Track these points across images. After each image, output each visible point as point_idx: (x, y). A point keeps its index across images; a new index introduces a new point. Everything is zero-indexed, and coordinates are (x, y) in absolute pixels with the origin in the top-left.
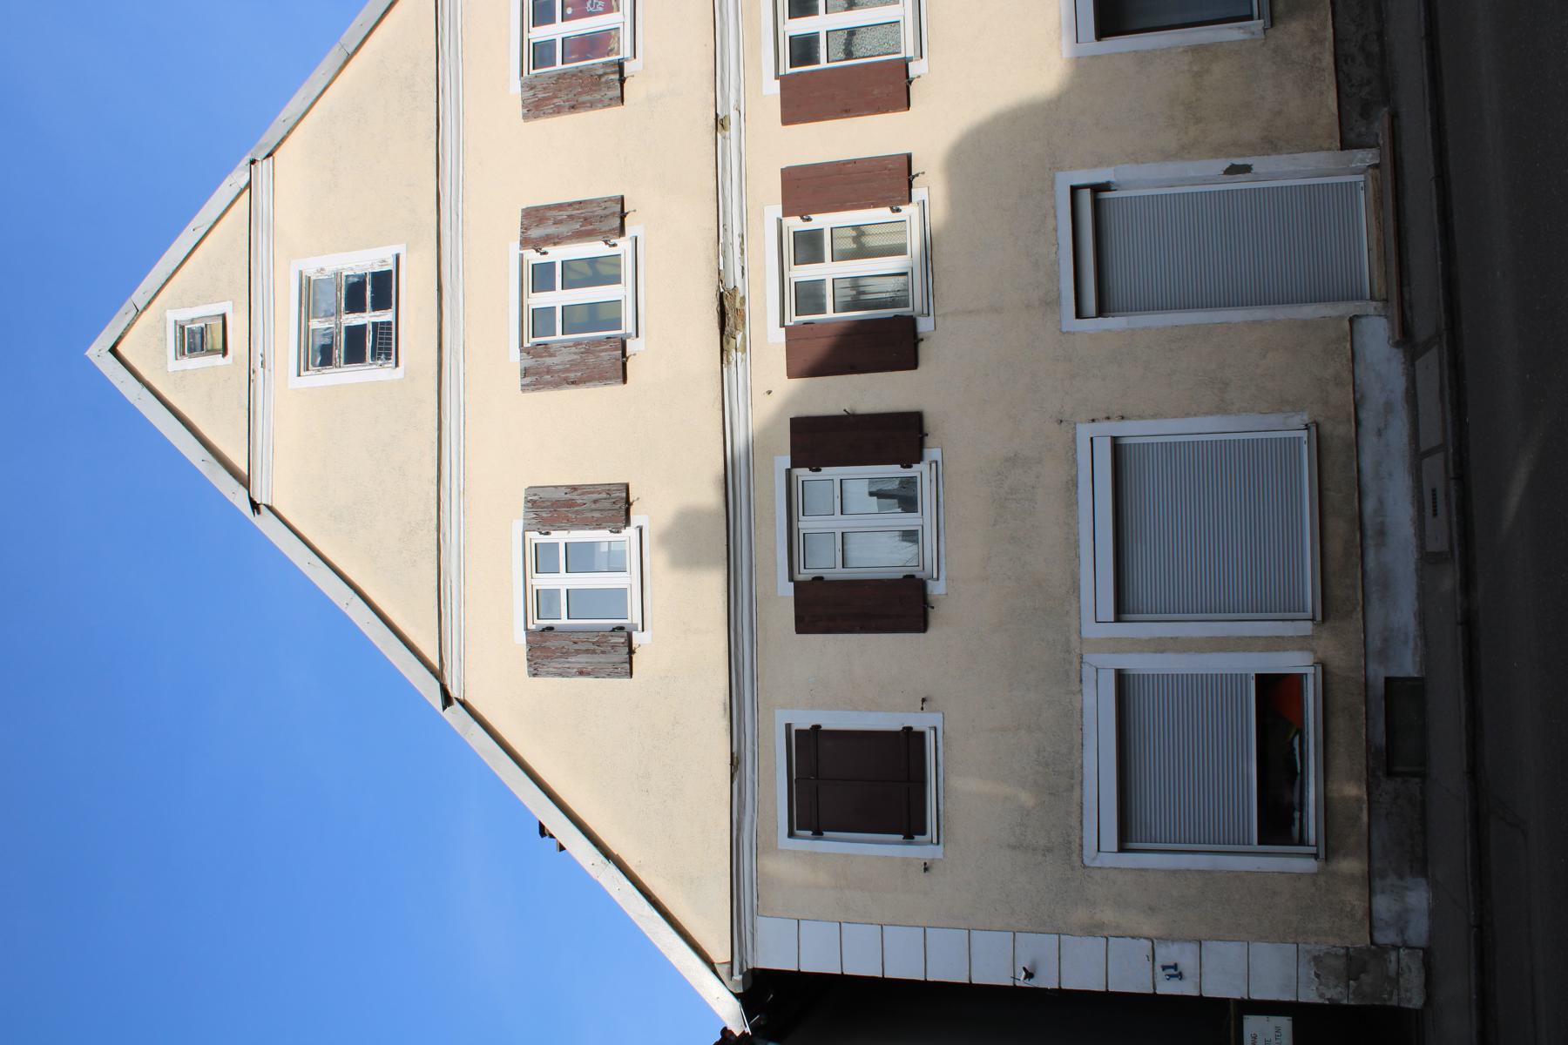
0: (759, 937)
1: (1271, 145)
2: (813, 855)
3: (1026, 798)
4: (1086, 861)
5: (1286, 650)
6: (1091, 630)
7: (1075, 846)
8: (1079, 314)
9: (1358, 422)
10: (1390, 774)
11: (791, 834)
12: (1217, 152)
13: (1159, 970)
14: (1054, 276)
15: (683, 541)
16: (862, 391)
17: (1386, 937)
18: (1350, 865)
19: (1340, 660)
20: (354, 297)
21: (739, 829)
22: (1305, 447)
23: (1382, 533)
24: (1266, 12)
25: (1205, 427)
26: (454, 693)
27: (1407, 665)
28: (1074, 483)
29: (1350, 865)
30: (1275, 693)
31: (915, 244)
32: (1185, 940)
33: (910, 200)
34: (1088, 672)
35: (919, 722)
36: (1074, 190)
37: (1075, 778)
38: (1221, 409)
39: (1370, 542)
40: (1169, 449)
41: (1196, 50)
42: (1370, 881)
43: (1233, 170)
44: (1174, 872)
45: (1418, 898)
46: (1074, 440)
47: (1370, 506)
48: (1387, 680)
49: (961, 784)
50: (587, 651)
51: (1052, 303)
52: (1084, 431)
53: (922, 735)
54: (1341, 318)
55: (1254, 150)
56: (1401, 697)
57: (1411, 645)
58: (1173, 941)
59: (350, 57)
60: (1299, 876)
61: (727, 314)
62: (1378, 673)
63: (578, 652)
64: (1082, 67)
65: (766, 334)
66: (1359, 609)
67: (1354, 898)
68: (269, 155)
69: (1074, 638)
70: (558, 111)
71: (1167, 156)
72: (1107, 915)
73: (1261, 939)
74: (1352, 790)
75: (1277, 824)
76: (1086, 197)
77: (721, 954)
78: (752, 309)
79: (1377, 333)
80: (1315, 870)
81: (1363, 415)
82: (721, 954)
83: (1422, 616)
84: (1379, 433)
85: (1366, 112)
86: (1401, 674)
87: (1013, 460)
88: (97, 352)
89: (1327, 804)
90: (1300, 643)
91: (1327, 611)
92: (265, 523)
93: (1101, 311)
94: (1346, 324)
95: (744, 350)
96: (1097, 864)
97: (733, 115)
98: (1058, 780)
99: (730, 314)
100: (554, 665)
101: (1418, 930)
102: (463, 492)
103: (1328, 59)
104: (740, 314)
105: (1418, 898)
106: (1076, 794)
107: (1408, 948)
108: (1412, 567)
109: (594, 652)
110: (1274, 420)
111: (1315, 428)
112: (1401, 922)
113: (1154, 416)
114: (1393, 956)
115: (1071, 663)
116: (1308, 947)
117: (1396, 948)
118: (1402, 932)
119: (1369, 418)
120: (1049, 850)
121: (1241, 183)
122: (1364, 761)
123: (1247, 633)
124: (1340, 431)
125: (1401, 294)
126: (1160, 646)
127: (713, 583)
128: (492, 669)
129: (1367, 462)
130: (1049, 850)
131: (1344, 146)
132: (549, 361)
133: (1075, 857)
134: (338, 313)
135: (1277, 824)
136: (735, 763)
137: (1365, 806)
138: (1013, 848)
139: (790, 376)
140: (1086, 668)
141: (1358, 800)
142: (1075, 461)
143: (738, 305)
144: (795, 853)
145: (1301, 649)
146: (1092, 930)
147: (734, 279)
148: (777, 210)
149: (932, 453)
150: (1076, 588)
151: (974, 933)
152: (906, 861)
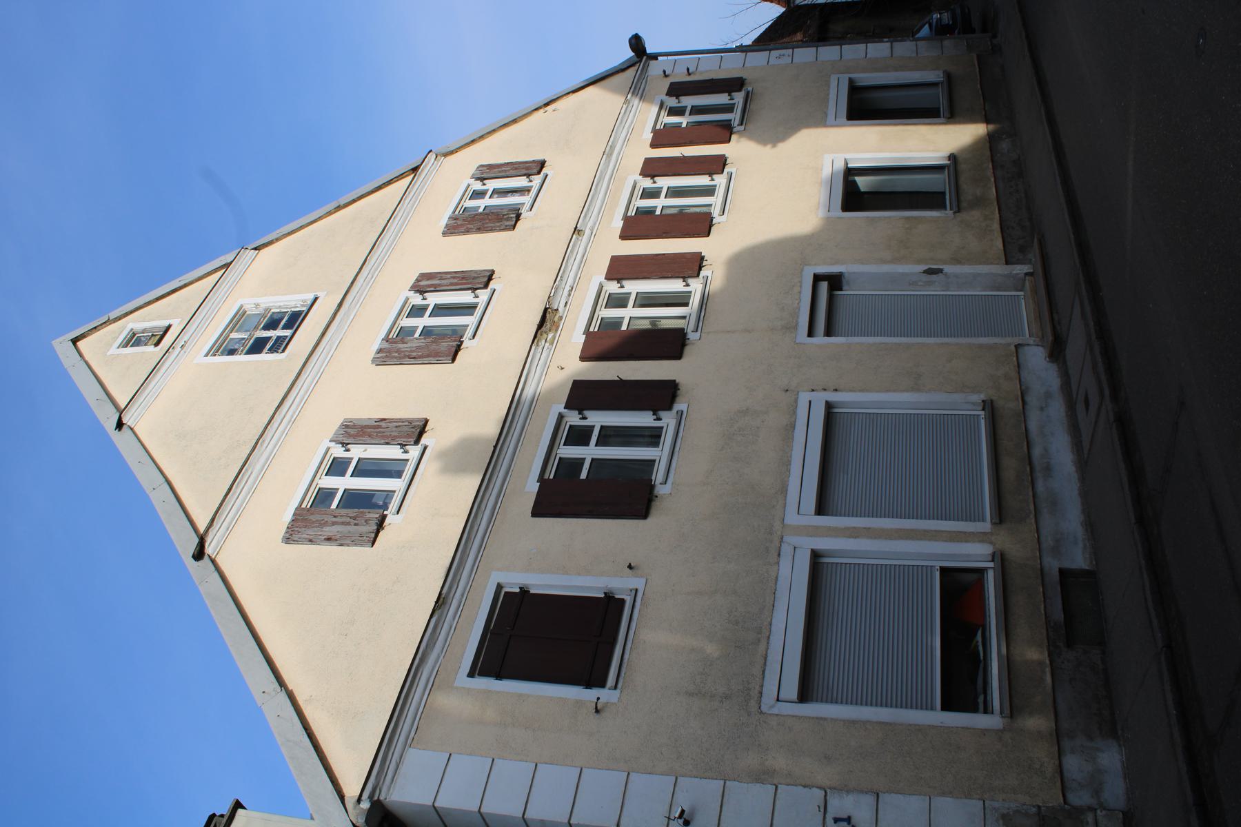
0: (403, 769)
1: (957, 261)
2: (488, 693)
3: (712, 649)
4: (764, 708)
5: (967, 541)
6: (792, 518)
7: (755, 693)
8: (811, 333)
9: (1024, 403)
10: (1069, 645)
11: (471, 675)
12: (919, 262)
13: (830, 821)
14: (795, 314)
15: (455, 461)
16: (634, 371)
17: (1080, 798)
18: (1037, 723)
19: (1016, 550)
20: (272, 324)
21: (422, 661)
22: (983, 422)
23: (1048, 469)
24: (955, 204)
25: (901, 400)
26: (209, 550)
27: (1078, 559)
28: (792, 426)
29: (1037, 723)
30: (959, 588)
31: (695, 301)
32: (861, 792)
33: (698, 275)
34: (786, 549)
35: (620, 585)
36: (817, 278)
37: (763, 633)
38: (916, 388)
39: (1039, 475)
40: (873, 419)
41: (907, 218)
42: (1058, 736)
43: (930, 272)
44: (853, 722)
45: (1111, 758)
46: (796, 401)
47: (1037, 452)
48: (1062, 572)
49: (655, 645)
50: (343, 523)
51: (792, 328)
52: (804, 398)
53: (622, 601)
54: (1009, 345)
55: (945, 263)
56: (1076, 608)
57: (1081, 545)
58: (848, 792)
59: (339, 208)
60: (984, 732)
61: (546, 321)
62: (1053, 565)
63: (334, 523)
64: (829, 222)
65: (572, 336)
66: (1032, 516)
67: (1042, 754)
68: (255, 249)
69: (777, 525)
70: (468, 231)
71: (883, 261)
72: (779, 761)
73: (943, 794)
74: (1033, 654)
75: (961, 689)
76: (824, 286)
77: (352, 789)
78: (565, 325)
79: (1036, 357)
80: (1001, 726)
81: (1028, 399)
82: (352, 789)
83: (1090, 525)
84: (1042, 409)
85: (1022, 249)
86: (1074, 566)
87: (745, 412)
88: (62, 346)
89: (1009, 665)
90: (981, 537)
91: (1001, 515)
92: (121, 440)
93: (829, 332)
94: (1013, 348)
95: (552, 343)
96: (775, 711)
97: (587, 232)
98: (747, 635)
99: (548, 324)
100: (311, 532)
101: (1115, 791)
102: (293, 422)
103: (996, 226)
104: (556, 326)
105: (1111, 758)
106: (762, 647)
107: (1104, 809)
108: (1076, 492)
109: (348, 524)
110: (957, 397)
111: (989, 406)
112: (1095, 783)
113: (862, 391)
114: (1090, 818)
115: (772, 542)
116: (996, 804)
117: (1092, 809)
118: (1097, 793)
119: (1032, 400)
120: (727, 697)
121: (935, 290)
122: (1044, 631)
123: (933, 528)
124: (1009, 406)
125: (1052, 319)
126: (854, 533)
127: (471, 483)
128: (254, 549)
129: (1033, 425)
130: (727, 697)
131: (1007, 263)
132: (401, 346)
133: (753, 703)
134: (256, 328)
135: (961, 689)
136: (441, 602)
137: (1048, 670)
138: (690, 694)
139: (583, 358)
140: (784, 547)
141: (1041, 663)
142: (794, 413)
143: (556, 319)
144: (469, 691)
145: (982, 541)
146: (762, 776)
147: (559, 303)
148: (601, 277)
149: (680, 406)
150: (784, 490)
151: (633, 776)
152: (579, 704)
